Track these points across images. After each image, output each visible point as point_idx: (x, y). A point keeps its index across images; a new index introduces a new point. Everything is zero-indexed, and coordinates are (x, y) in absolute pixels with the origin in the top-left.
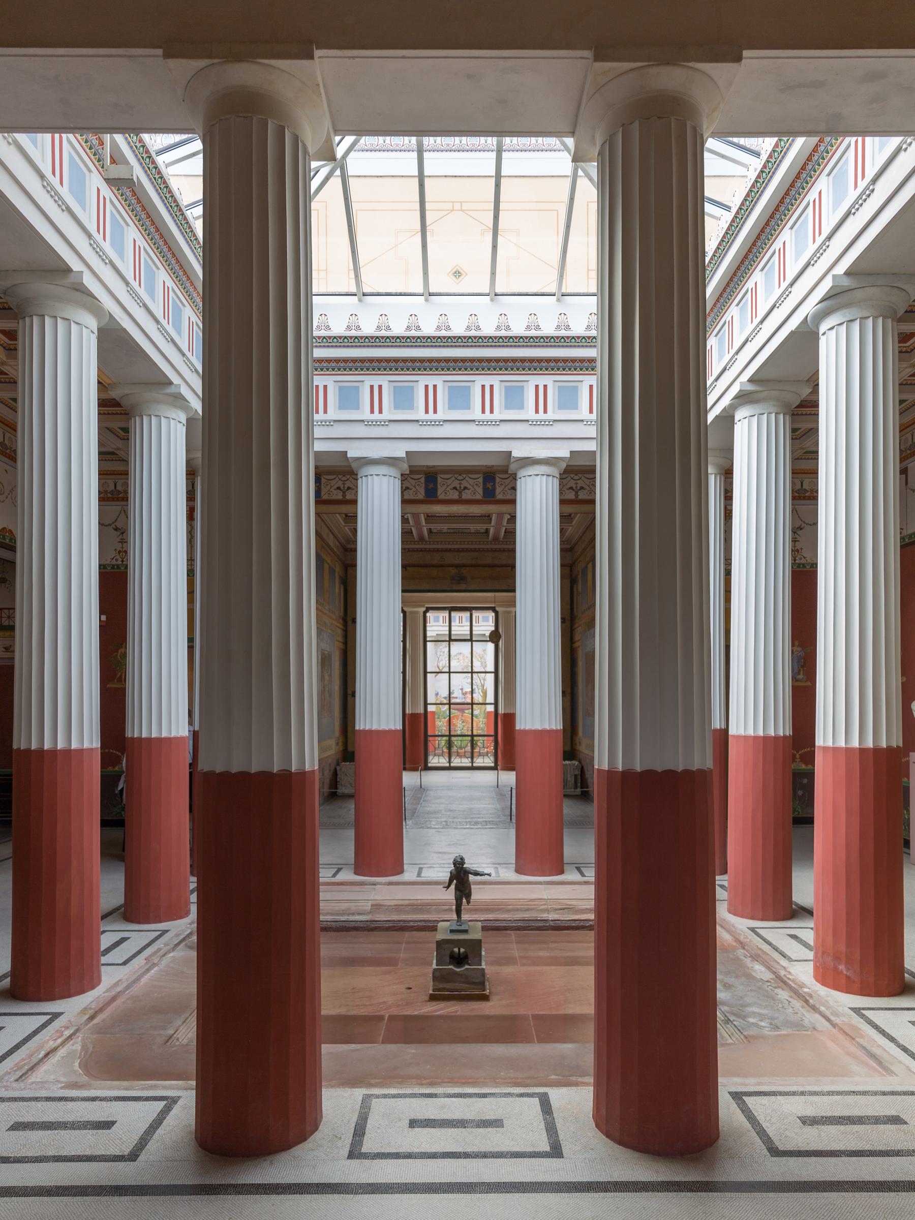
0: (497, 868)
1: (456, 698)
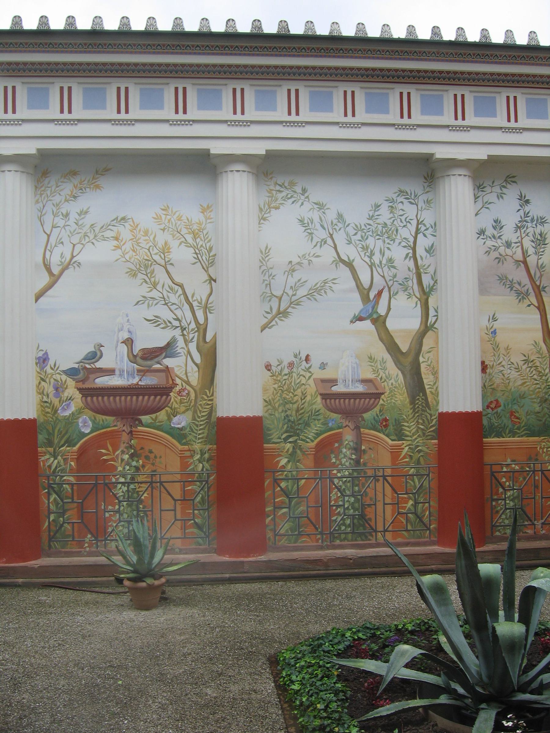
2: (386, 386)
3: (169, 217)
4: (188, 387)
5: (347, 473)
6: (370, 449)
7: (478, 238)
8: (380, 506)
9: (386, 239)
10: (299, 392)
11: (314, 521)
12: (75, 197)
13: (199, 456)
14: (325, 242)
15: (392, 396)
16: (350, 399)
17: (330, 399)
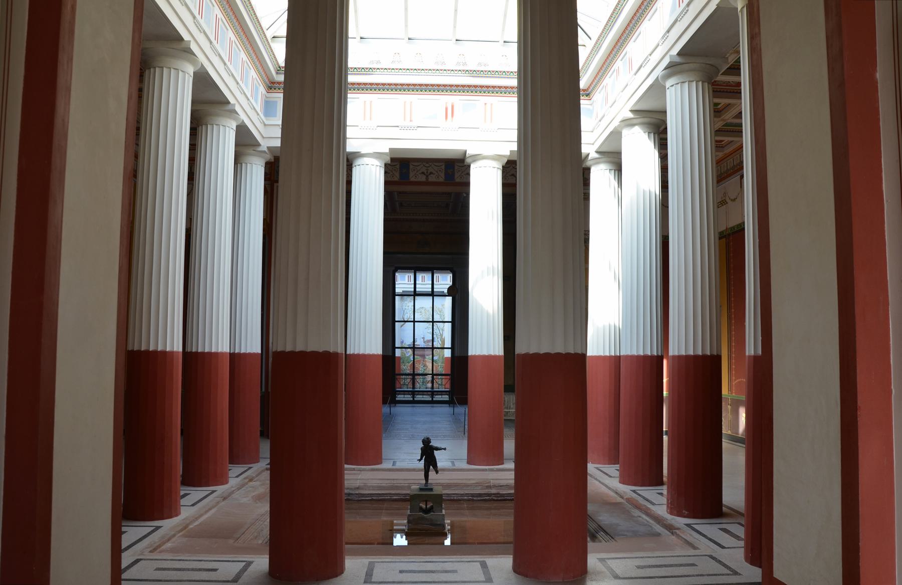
0: (453, 462)
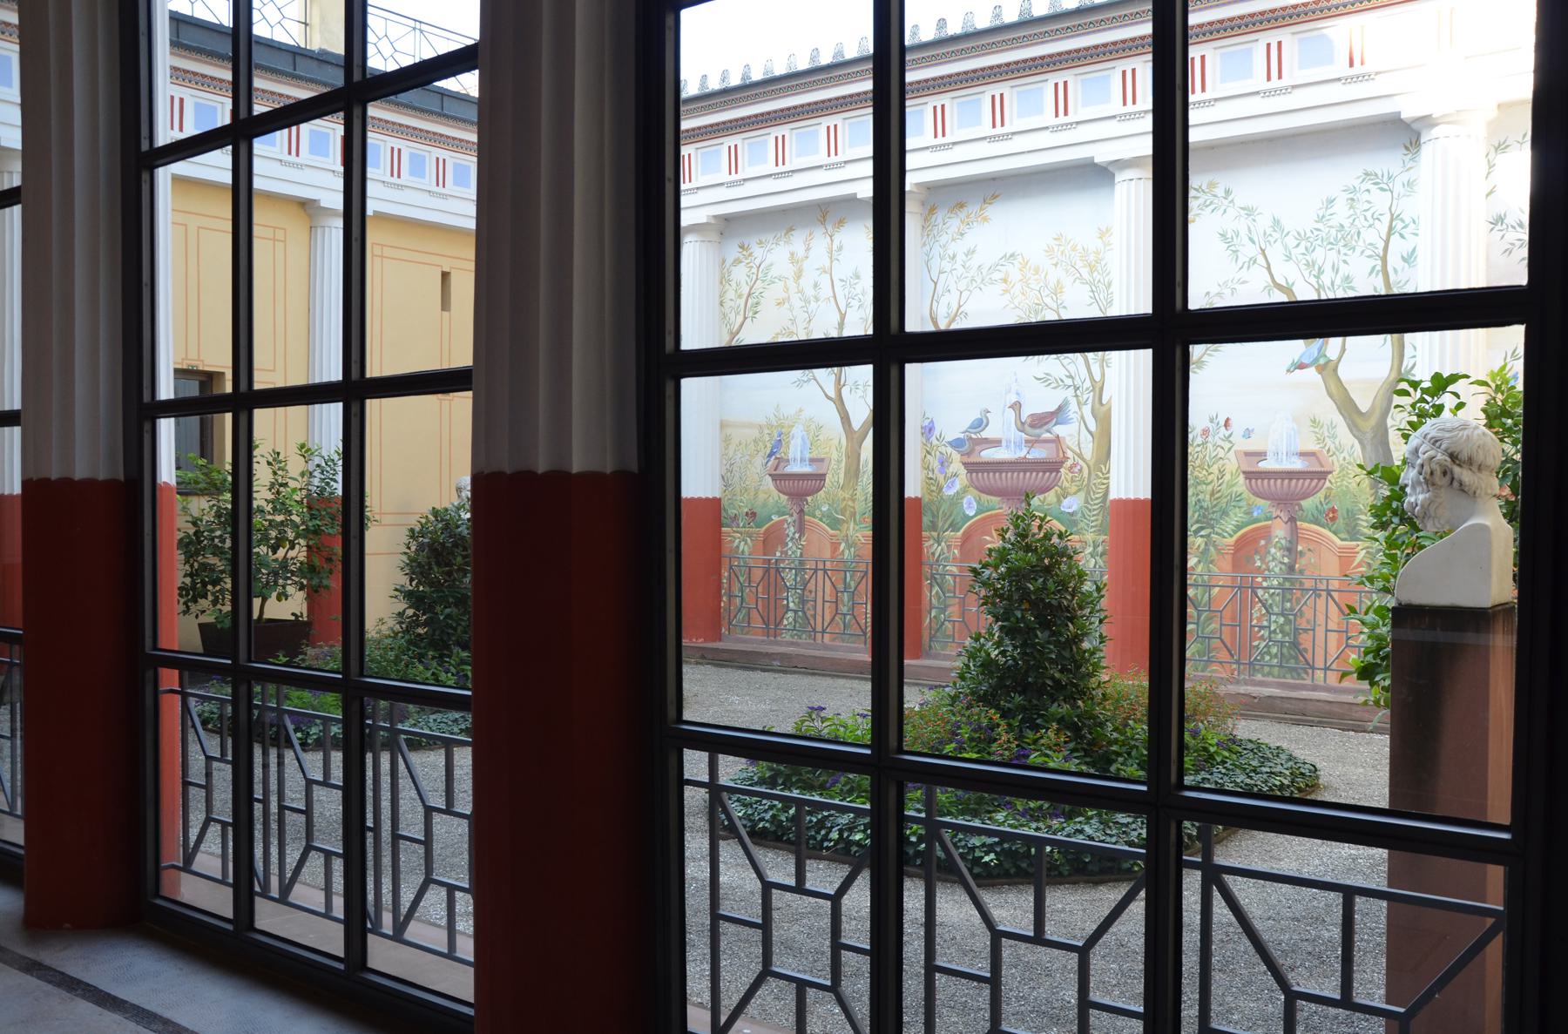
1: (996, 443)
2: (1335, 463)
3: (1062, 248)
4: (1081, 462)
5: (1275, 582)
6: (1309, 550)
7: (1492, 230)
8: (1320, 632)
9: (1341, 249)
10: (1215, 469)
11: (1229, 645)
12: (962, 234)
13: (1091, 549)
14: (1255, 262)
15: (1344, 476)
16: (1283, 479)
17: (1257, 479)
